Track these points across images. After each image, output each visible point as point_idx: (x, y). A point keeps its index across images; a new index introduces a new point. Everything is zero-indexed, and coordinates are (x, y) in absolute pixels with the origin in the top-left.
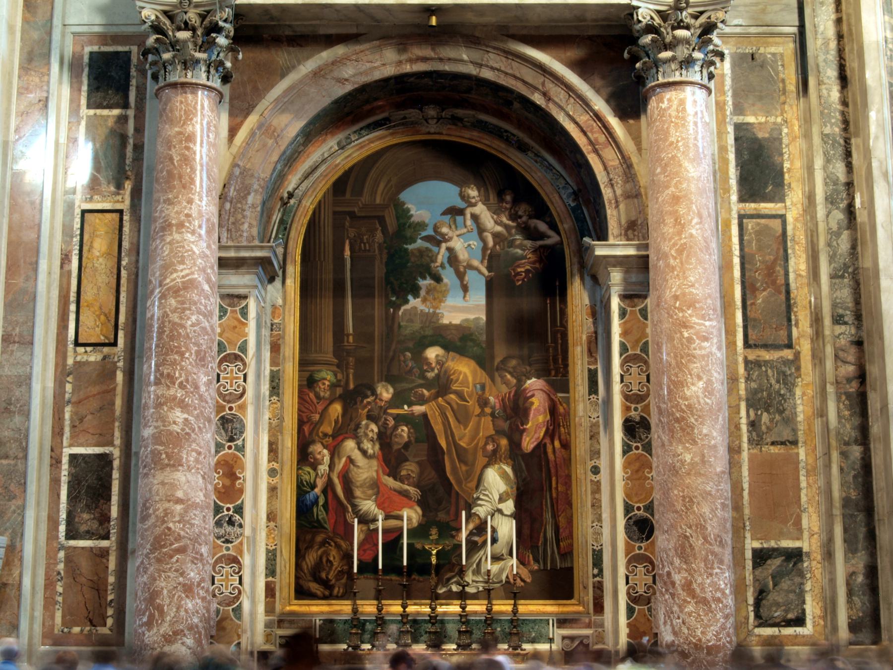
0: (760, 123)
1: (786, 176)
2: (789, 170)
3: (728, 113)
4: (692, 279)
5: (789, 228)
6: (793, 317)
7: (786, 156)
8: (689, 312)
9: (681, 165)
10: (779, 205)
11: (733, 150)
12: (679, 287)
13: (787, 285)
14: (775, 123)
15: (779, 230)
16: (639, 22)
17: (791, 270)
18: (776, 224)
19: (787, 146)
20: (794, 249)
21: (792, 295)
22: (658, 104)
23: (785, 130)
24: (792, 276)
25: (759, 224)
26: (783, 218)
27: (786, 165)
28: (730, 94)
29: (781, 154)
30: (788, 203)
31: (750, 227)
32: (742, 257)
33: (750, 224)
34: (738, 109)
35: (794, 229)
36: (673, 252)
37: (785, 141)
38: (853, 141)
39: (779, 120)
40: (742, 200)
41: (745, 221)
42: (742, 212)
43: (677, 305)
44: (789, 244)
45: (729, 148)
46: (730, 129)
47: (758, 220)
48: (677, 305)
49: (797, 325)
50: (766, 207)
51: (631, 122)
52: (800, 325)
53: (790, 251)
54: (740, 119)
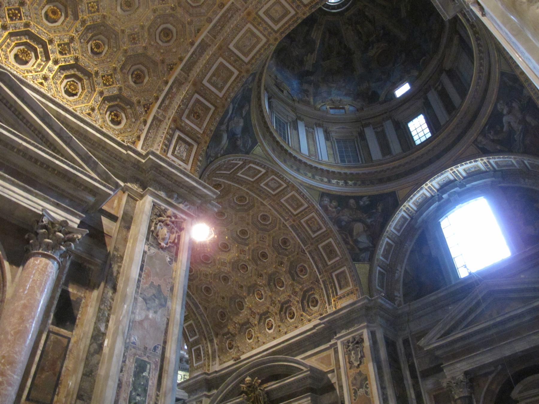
0: (74, 294)
1: (77, 321)
2: (79, 319)
3: (61, 283)
4: (17, 349)
5: (71, 345)
6: (57, 390)
7: (80, 312)
8: (8, 367)
9: (34, 292)
10: (70, 333)
11: (57, 300)
12: (8, 352)
13: (60, 373)
14: (80, 296)
15: (66, 344)
16: (42, 222)
17: (65, 365)
18: (65, 341)
19: (82, 308)
20: (69, 355)
21: (61, 379)
22: (34, 260)
23: (83, 301)
24: (64, 369)
25: (57, 338)
26: (69, 339)
27: (79, 316)
28: (65, 275)
29: (78, 310)
30: (74, 333)
31: (52, 337)
32: (43, 352)
33: (52, 337)
34: (66, 284)
35: (73, 346)
36: (12, 332)
37: (82, 305)
38: (111, 316)
39: (83, 295)
40: (53, 324)
41: (51, 334)
42: (51, 330)
43: (3, 361)
44: (68, 352)
45: (56, 298)
46: (60, 290)
47: (57, 336)
48: (3, 361)
49: (58, 395)
50: (63, 331)
51: (14, 267)
52: (59, 395)
53: (67, 356)
54: (65, 288)
